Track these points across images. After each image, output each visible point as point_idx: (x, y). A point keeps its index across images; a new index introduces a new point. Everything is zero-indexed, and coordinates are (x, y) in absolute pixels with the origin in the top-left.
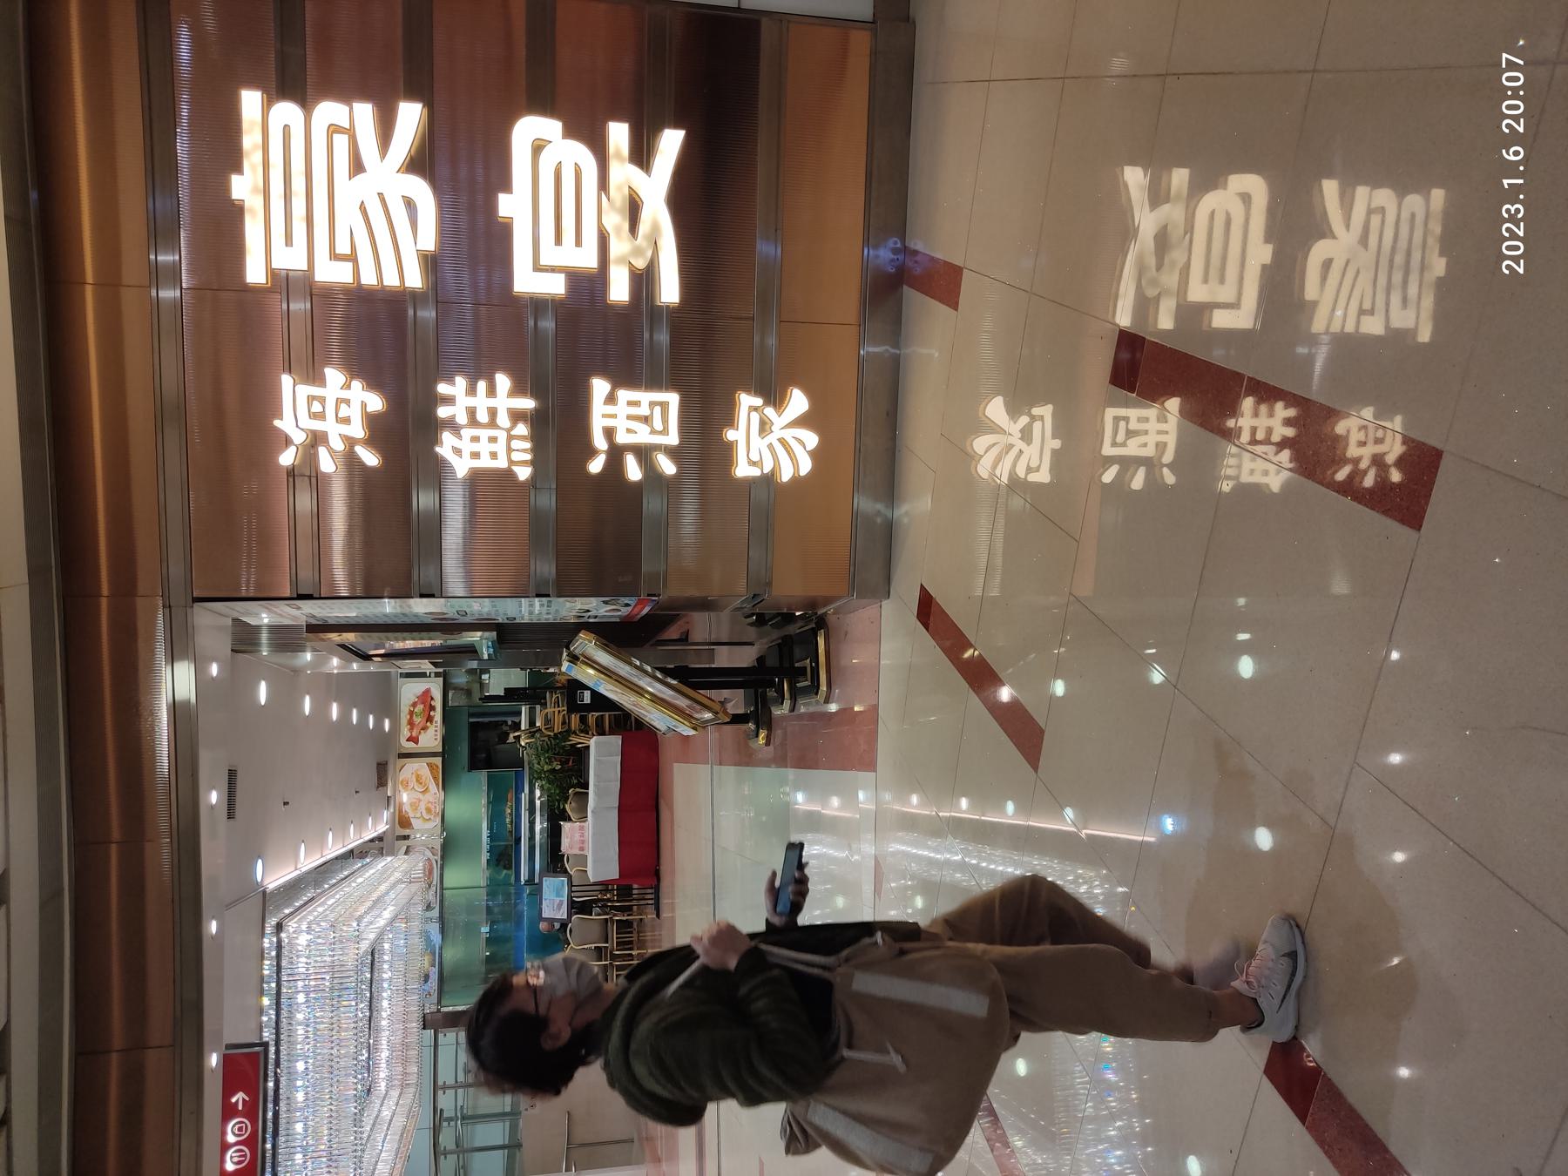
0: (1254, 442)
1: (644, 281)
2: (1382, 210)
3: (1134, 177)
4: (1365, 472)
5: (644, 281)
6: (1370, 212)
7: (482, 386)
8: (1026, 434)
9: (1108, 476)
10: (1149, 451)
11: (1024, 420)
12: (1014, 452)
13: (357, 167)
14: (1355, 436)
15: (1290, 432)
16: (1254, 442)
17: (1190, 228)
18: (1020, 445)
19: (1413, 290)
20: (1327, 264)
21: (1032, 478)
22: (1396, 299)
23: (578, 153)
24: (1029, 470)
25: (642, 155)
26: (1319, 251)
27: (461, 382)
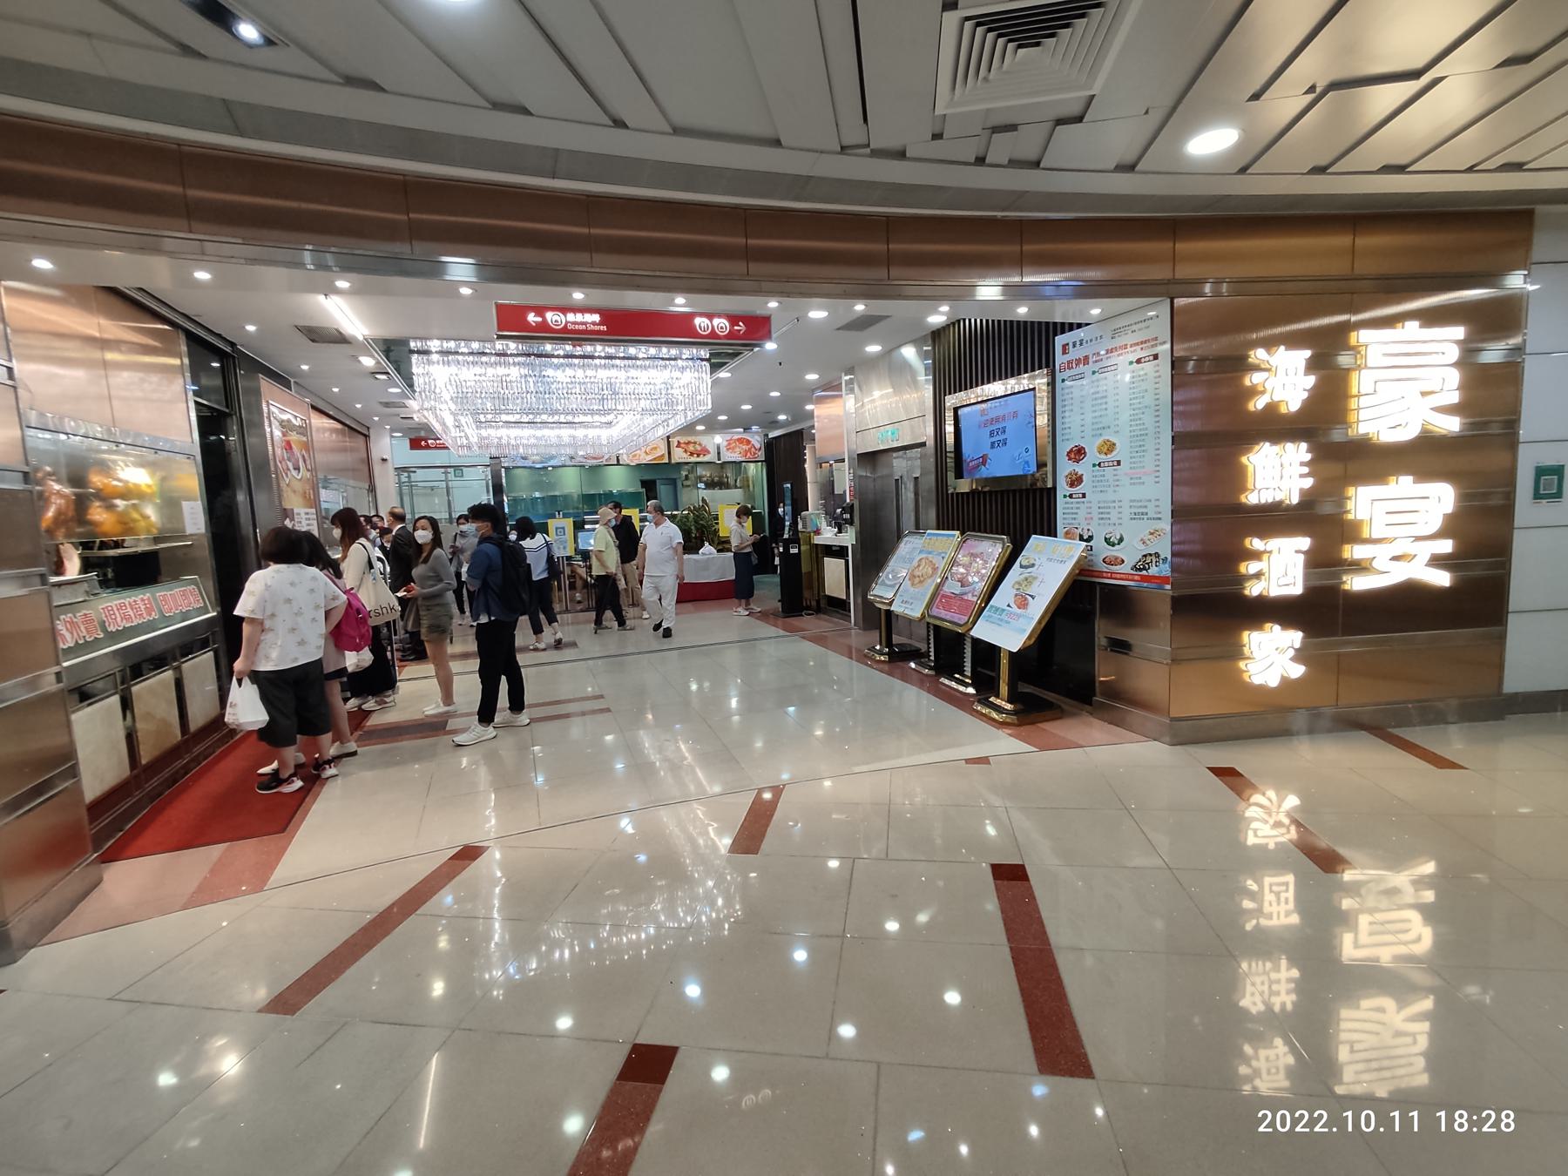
0: (1271, 982)
1: (1359, 567)
2: (1415, 1042)
3: (1429, 868)
4: (1250, 1066)
5: (1359, 567)
6: (1414, 1035)
7: (1306, 470)
8: (1278, 824)
9: (1252, 885)
10: (1267, 908)
11: (1286, 821)
12: (1266, 817)
13: (1424, 394)
14: (1271, 1053)
15: (1277, 1008)
16: (1271, 982)
17: (1401, 908)
18: (1271, 821)
19: (1366, 1077)
20: (1382, 1010)
21: (1250, 833)
22: (1360, 1067)
23: (1436, 524)
24: (1255, 831)
25: (1437, 561)
26: (1388, 1003)
27: (1308, 457)
